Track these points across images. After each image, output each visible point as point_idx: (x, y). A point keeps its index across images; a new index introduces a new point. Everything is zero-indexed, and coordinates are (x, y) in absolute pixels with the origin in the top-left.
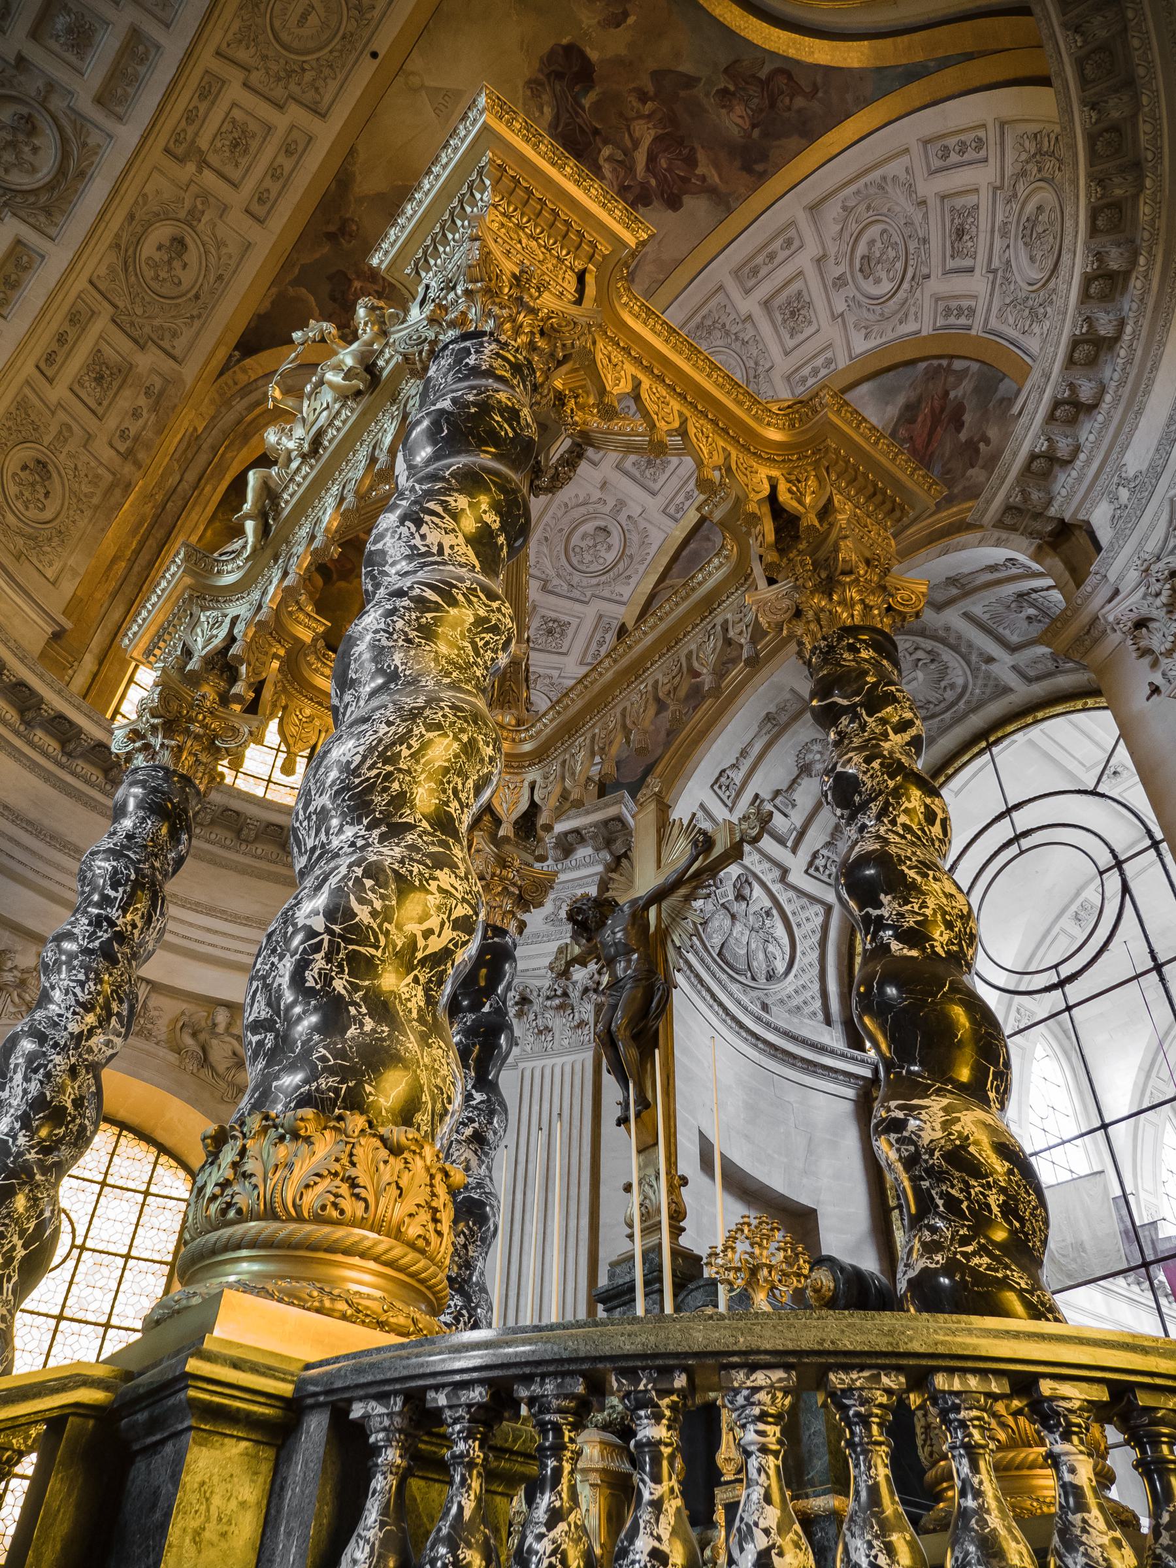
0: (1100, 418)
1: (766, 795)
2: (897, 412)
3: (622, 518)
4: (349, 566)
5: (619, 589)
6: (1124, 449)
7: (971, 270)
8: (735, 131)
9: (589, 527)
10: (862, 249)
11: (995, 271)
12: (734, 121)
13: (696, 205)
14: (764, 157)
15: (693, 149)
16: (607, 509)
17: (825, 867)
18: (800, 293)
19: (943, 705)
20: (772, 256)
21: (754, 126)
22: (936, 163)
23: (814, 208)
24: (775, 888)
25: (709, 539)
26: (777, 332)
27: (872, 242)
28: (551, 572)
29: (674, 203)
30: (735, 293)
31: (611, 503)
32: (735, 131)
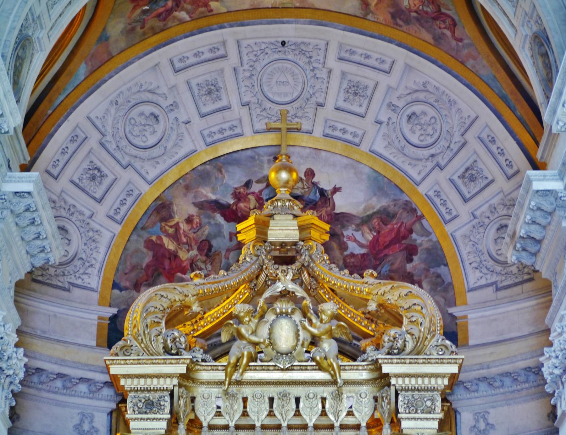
0: (493, 392)
2: (378, 207)
3: (172, 116)
5: (148, 166)
6: (493, 407)
7: (466, 200)
9: (148, 109)
10: (418, 108)
11: (475, 217)
14: (407, 22)
16: (165, 104)
18: (366, 87)
20: (367, 57)
21: (416, 12)
22: (484, 136)
25: (221, 172)
26: (339, 91)
27: (424, 113)
28: (109, 129)
31: (169, 101)
32: (406, 3)
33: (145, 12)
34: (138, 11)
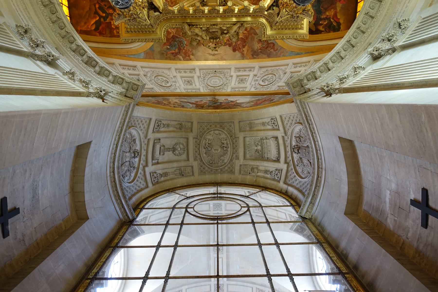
1: (162, 141)
4: (104, 33)
8: (256, 48)
9: (165, 79)
10: (265, 77)
12: (257, 46)
13: (238, 54)
14: (257, 55)
15: (246, 45)
17: (155, 178)
19: (216, 165)
23: (261, 67)
24: (141, 166)
29: (234, 50)
30: (233, 70)
32: (256, 48)
33: (168, 49)
34: (165, 47)
